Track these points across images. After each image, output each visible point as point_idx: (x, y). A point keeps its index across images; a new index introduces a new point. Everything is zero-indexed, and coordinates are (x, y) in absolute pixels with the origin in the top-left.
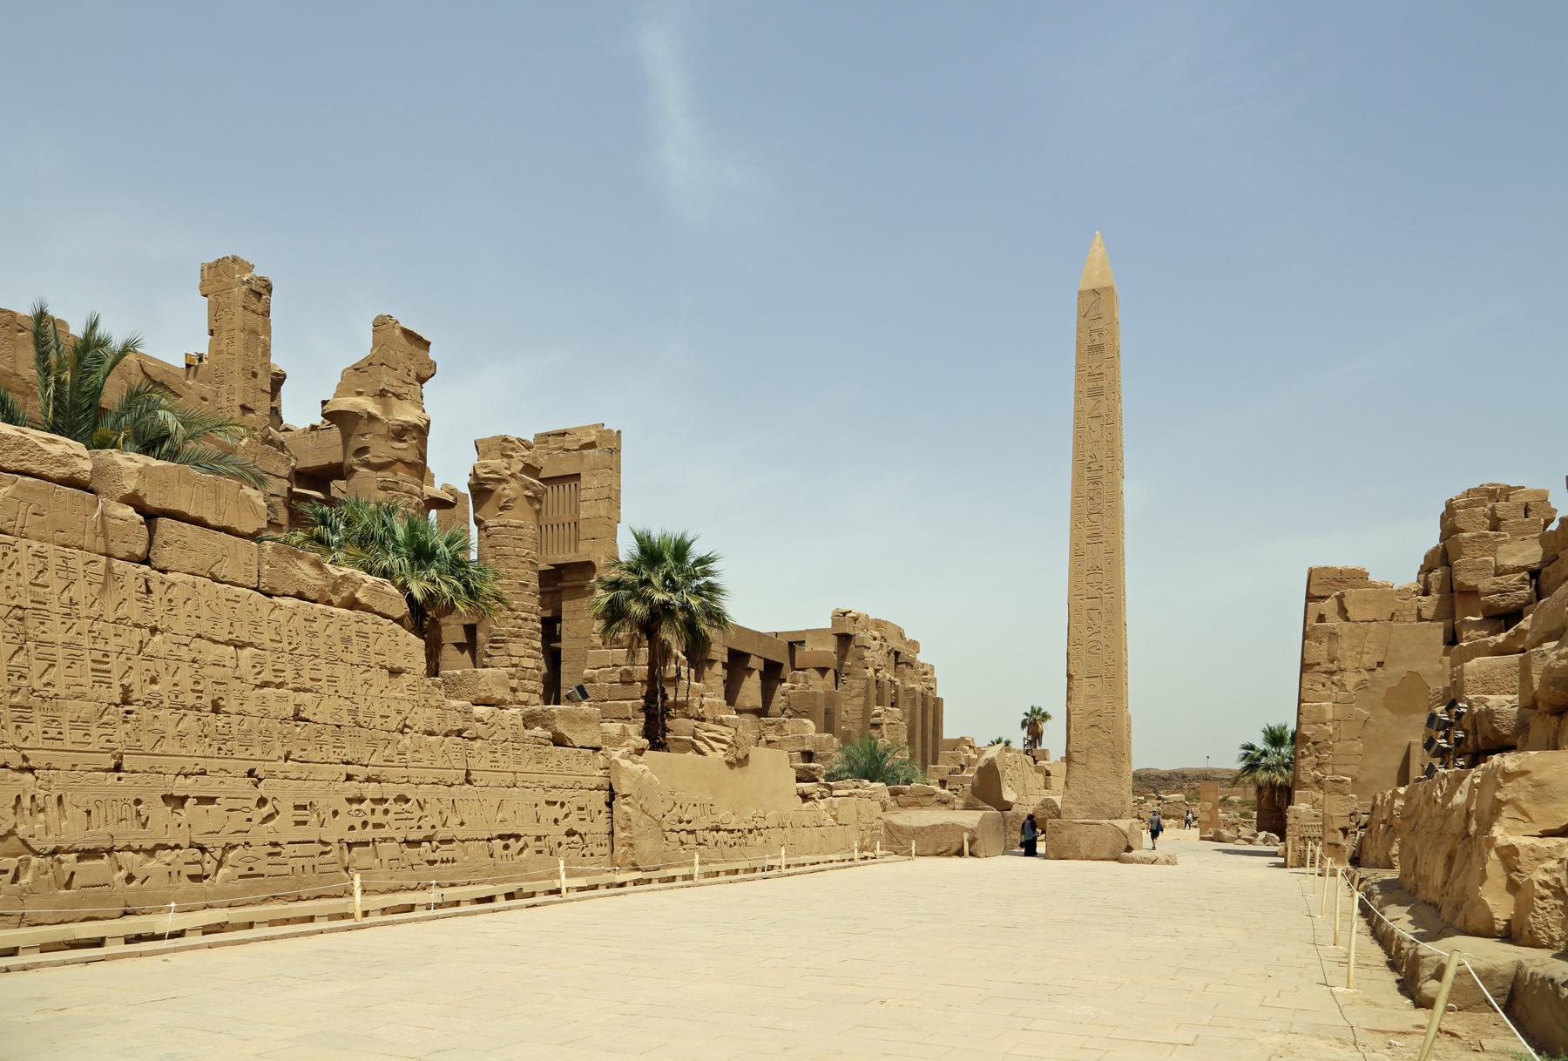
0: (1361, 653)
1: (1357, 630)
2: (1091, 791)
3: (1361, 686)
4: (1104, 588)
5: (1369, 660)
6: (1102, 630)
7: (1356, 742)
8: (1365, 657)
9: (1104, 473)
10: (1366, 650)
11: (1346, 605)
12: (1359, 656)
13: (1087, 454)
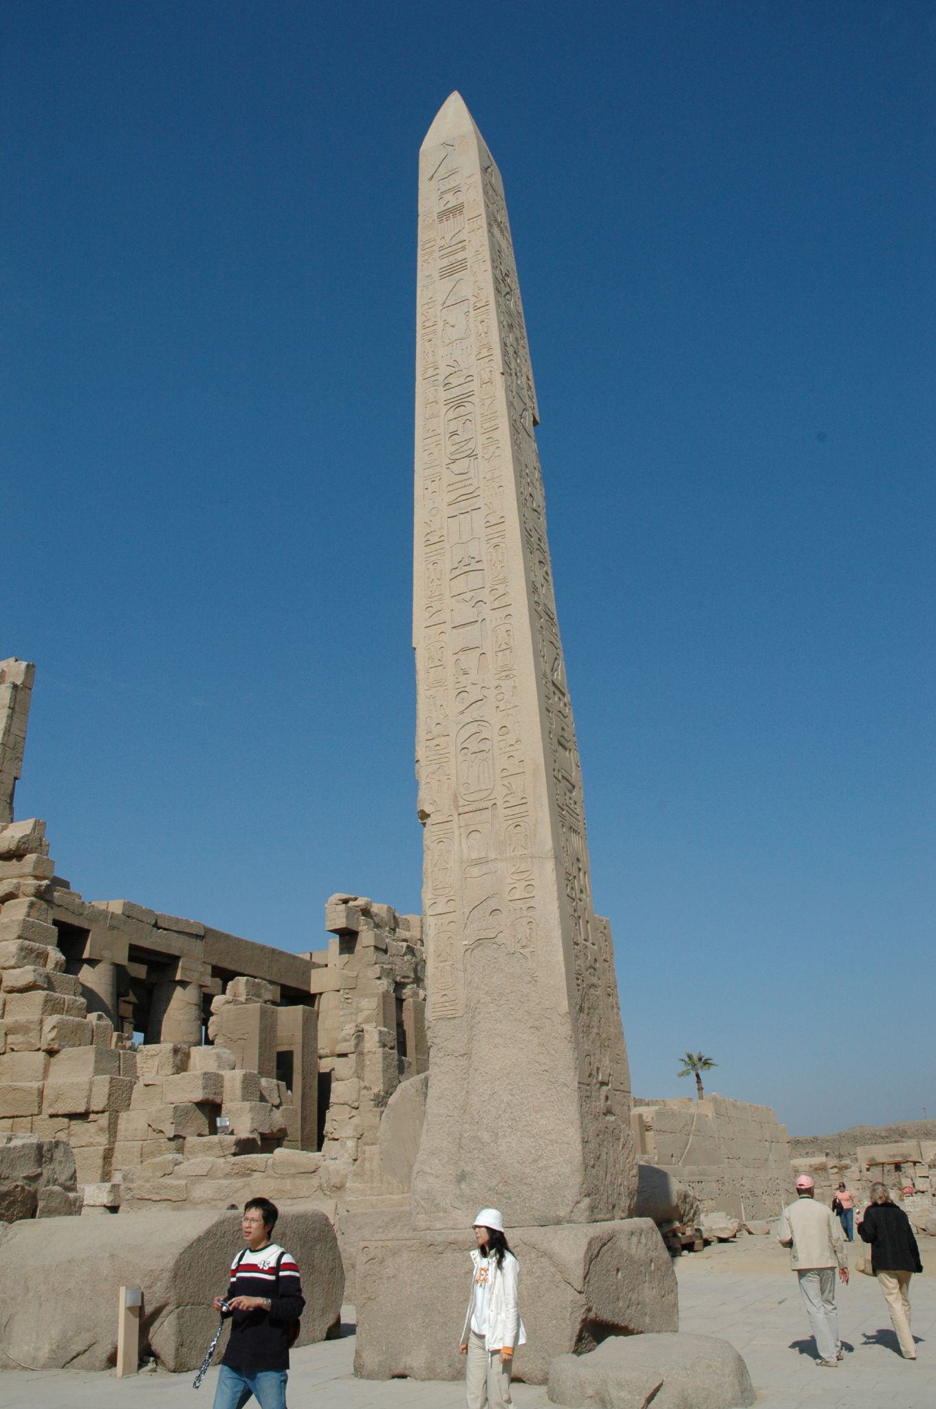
9: (475, 386)
13: (442, 365)
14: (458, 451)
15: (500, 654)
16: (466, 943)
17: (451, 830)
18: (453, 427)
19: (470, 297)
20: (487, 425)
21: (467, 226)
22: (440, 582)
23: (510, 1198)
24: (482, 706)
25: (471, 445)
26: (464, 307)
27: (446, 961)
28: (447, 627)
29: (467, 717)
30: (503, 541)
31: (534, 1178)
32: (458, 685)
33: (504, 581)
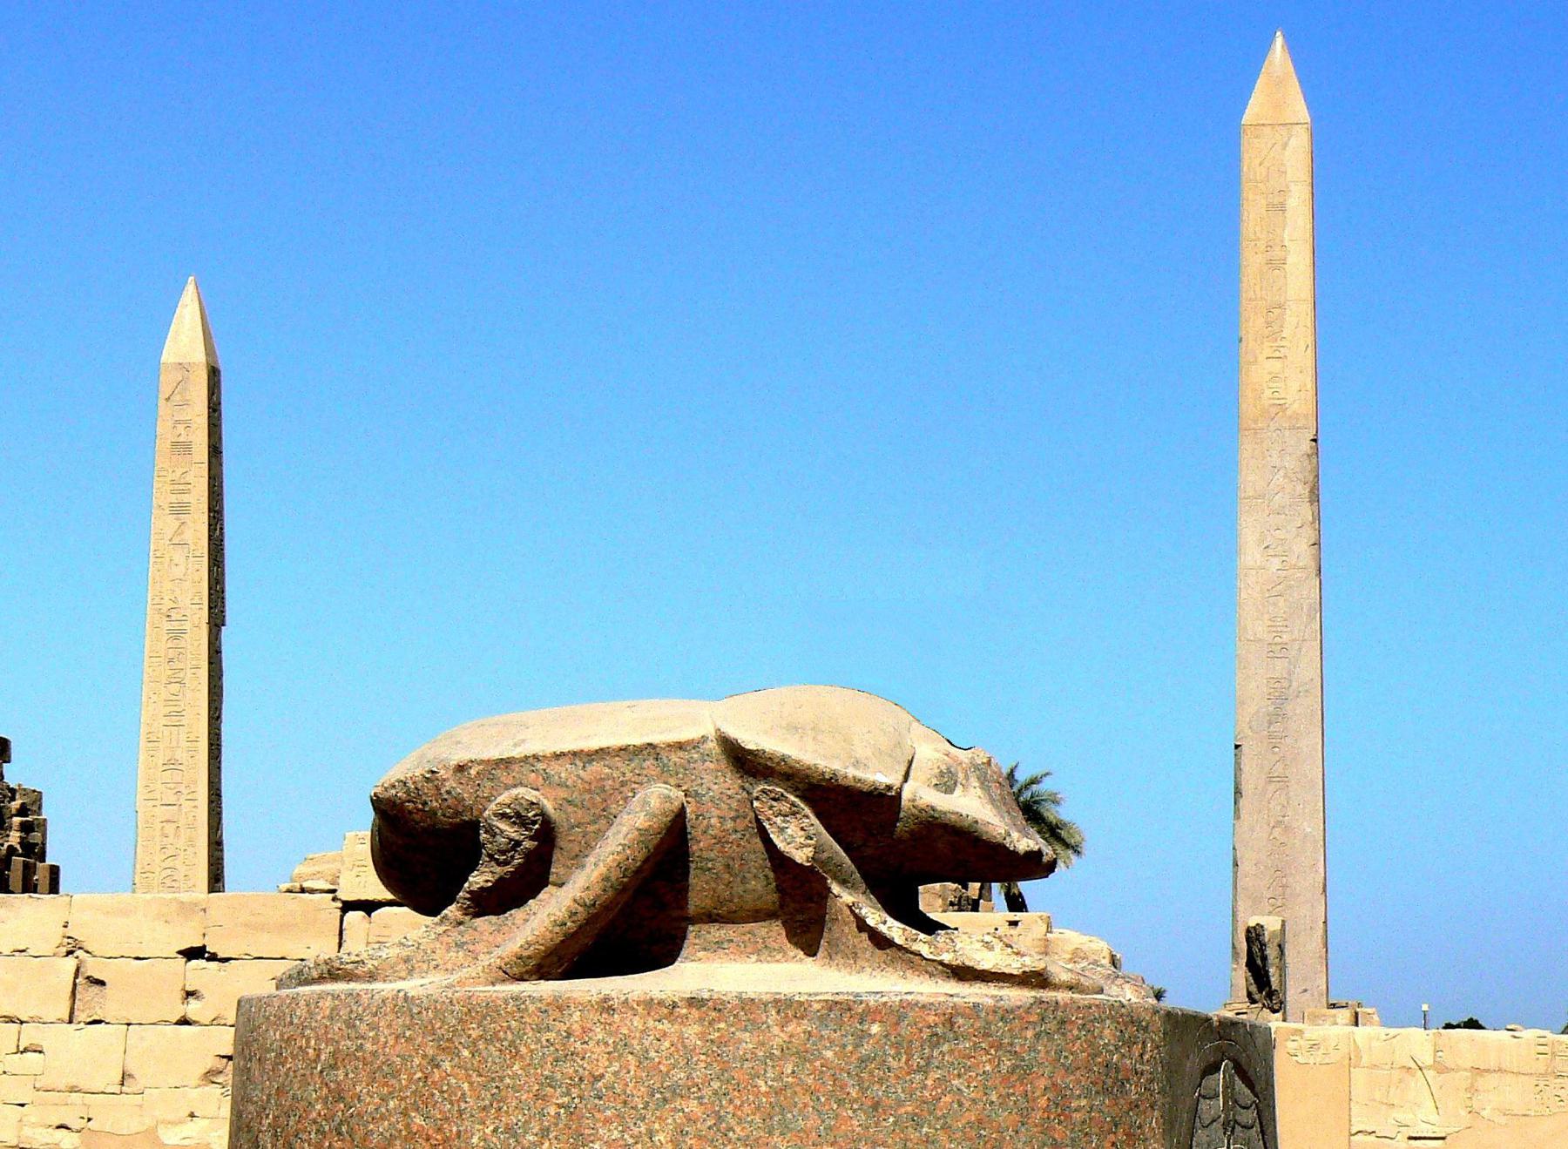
4: (185, 791)
9: (187, 626)
13: (166, 598)
18: (171, 653)
20: (194, 663)
25: (181, 675)
33: (195, 782)
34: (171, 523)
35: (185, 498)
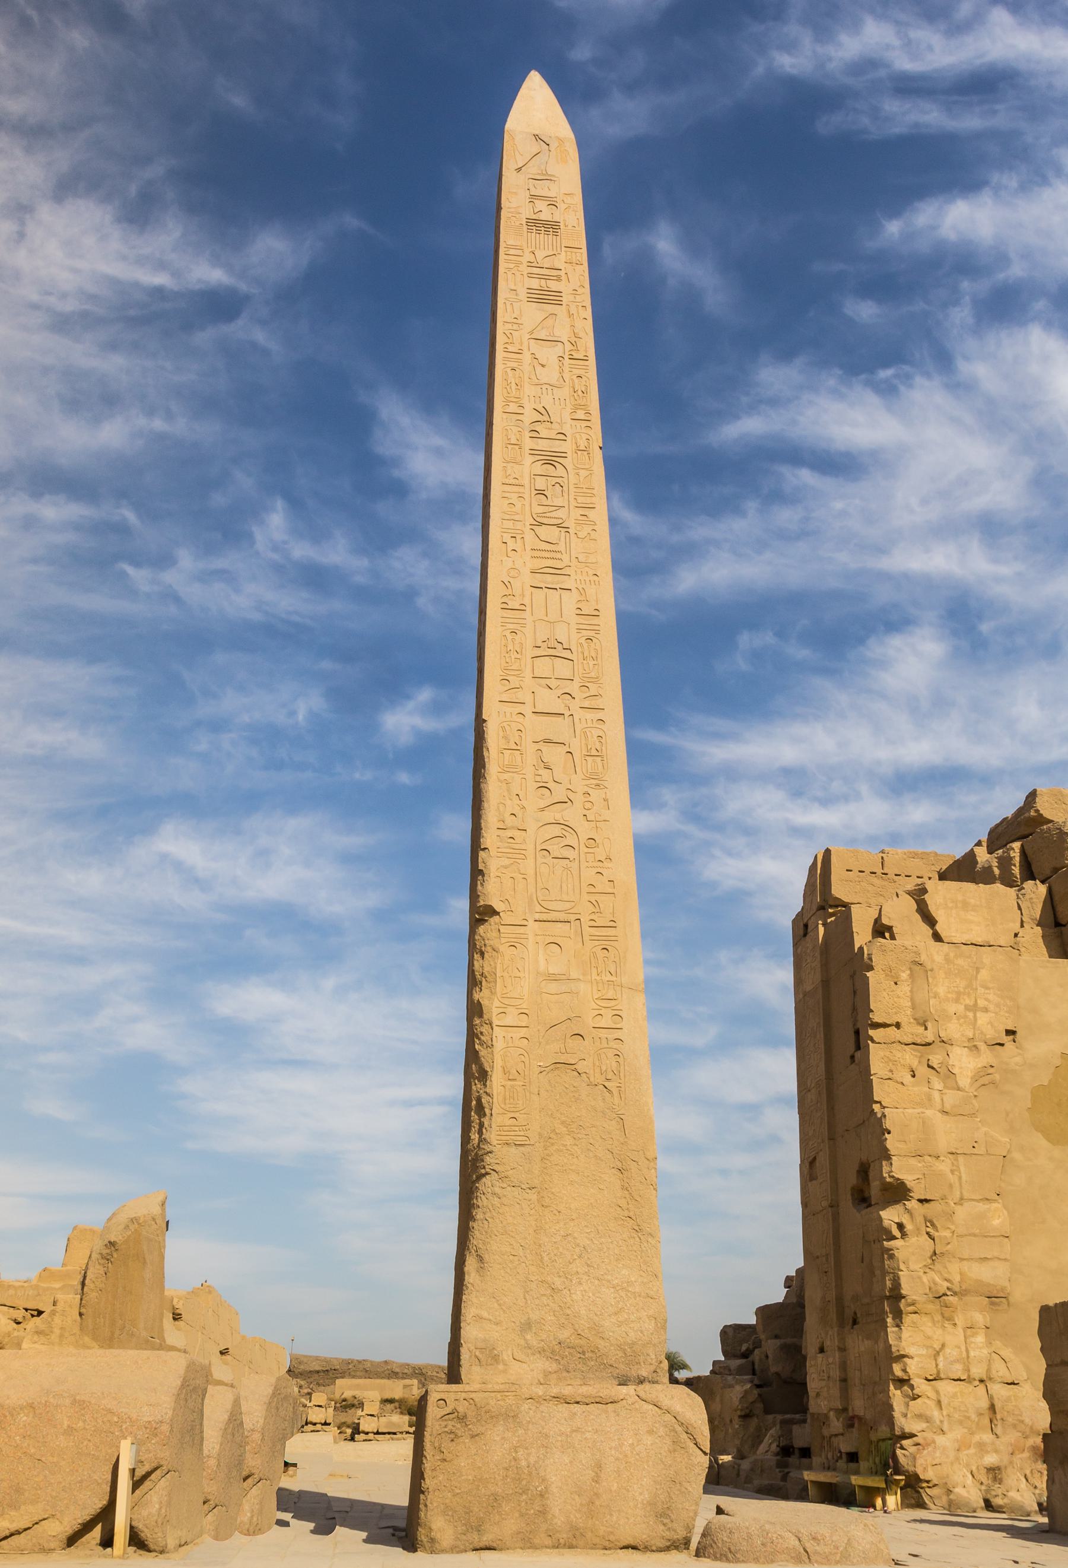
0: (974, 1008)
1: (960, 961)
2: (558, 1282)
3: (984, 1078)
5: (990, 1025)
6: (578, 799)
7: (995, 1205)
8: (983, 1019)
10: (981, 1003)
11: (932, 908)
12: (971, 1015)
14: (543, 515)
15: (589, 759)
16: (542, 1064)
17: (525, 936)
18: (541, 483)
19: (565, 339)
20: (580, 500)
21: (563, 253)
22: (519, 656)
23: (584, 1353)
24: (566, 809)
25: (561, 513)
26: (558, 349)
27: (515, 1080)
28: (527, 710)
29: (549, 816)
30: (596, 636)
31: (613, 1332)
32: (538, 778)
33: (596, 680)
34: (533, 314)
35: (553, 285)
